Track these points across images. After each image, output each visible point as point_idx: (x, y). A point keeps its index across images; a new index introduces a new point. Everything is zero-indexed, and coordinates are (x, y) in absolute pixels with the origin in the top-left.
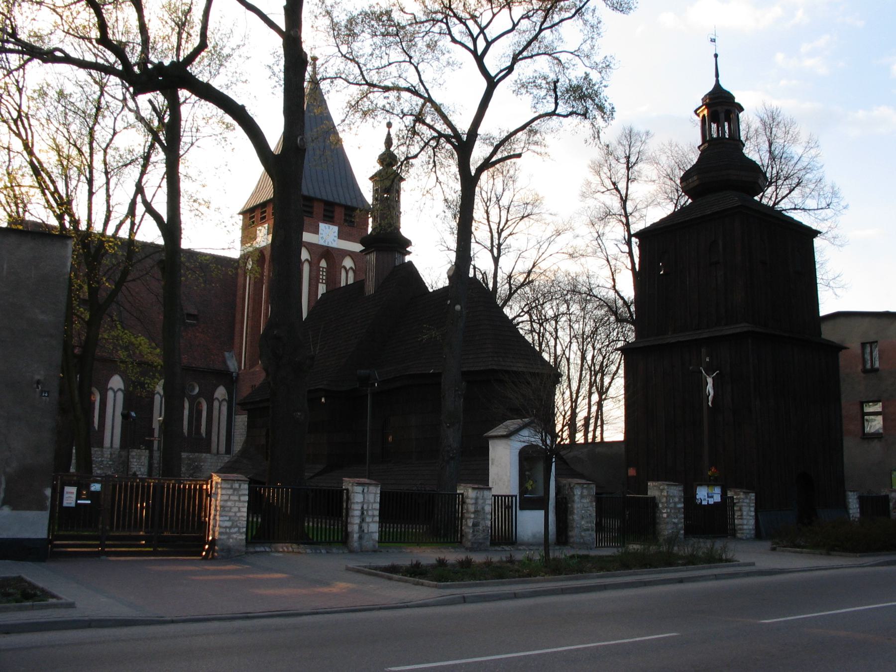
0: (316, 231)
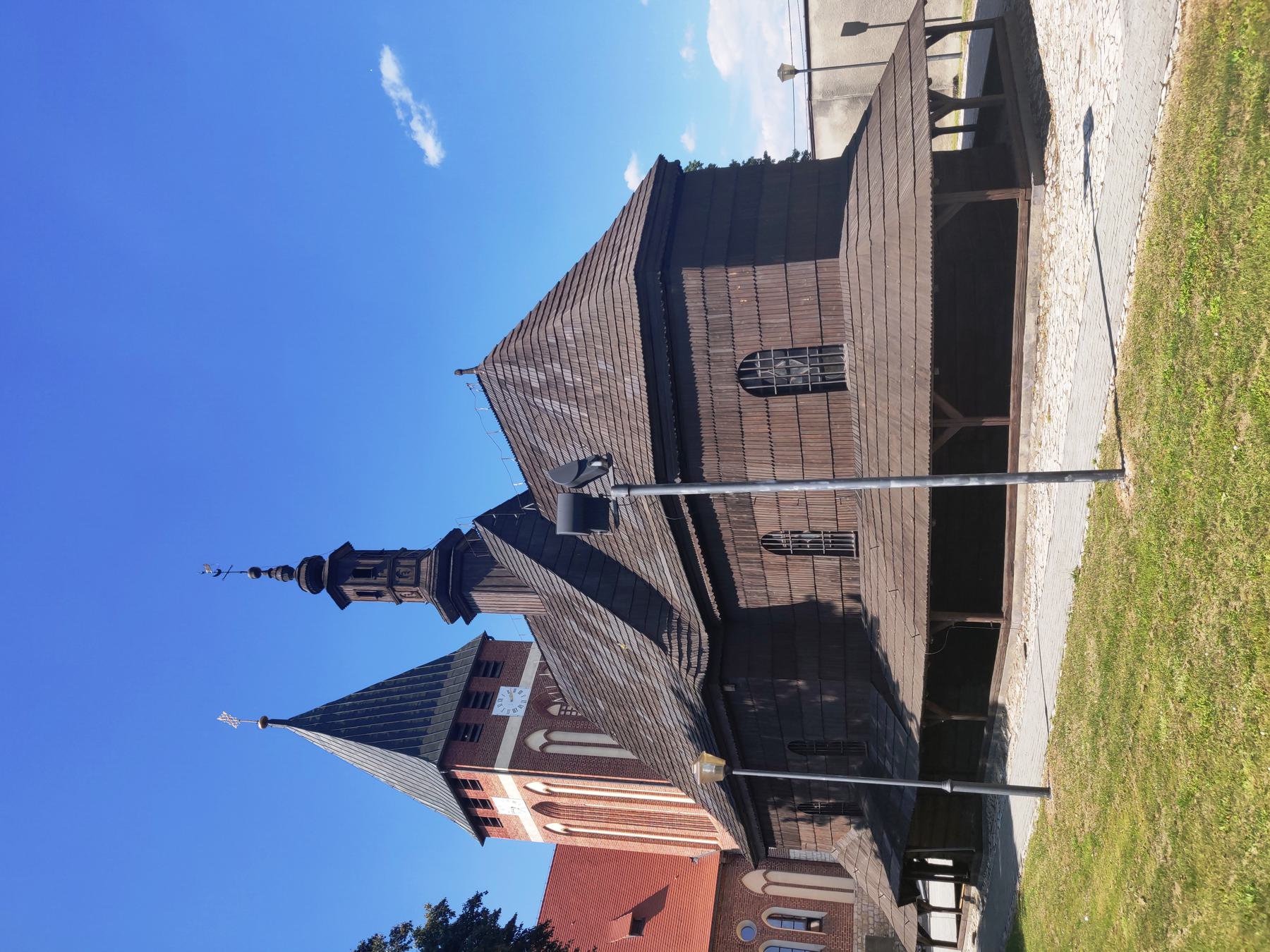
0: (504, 720)
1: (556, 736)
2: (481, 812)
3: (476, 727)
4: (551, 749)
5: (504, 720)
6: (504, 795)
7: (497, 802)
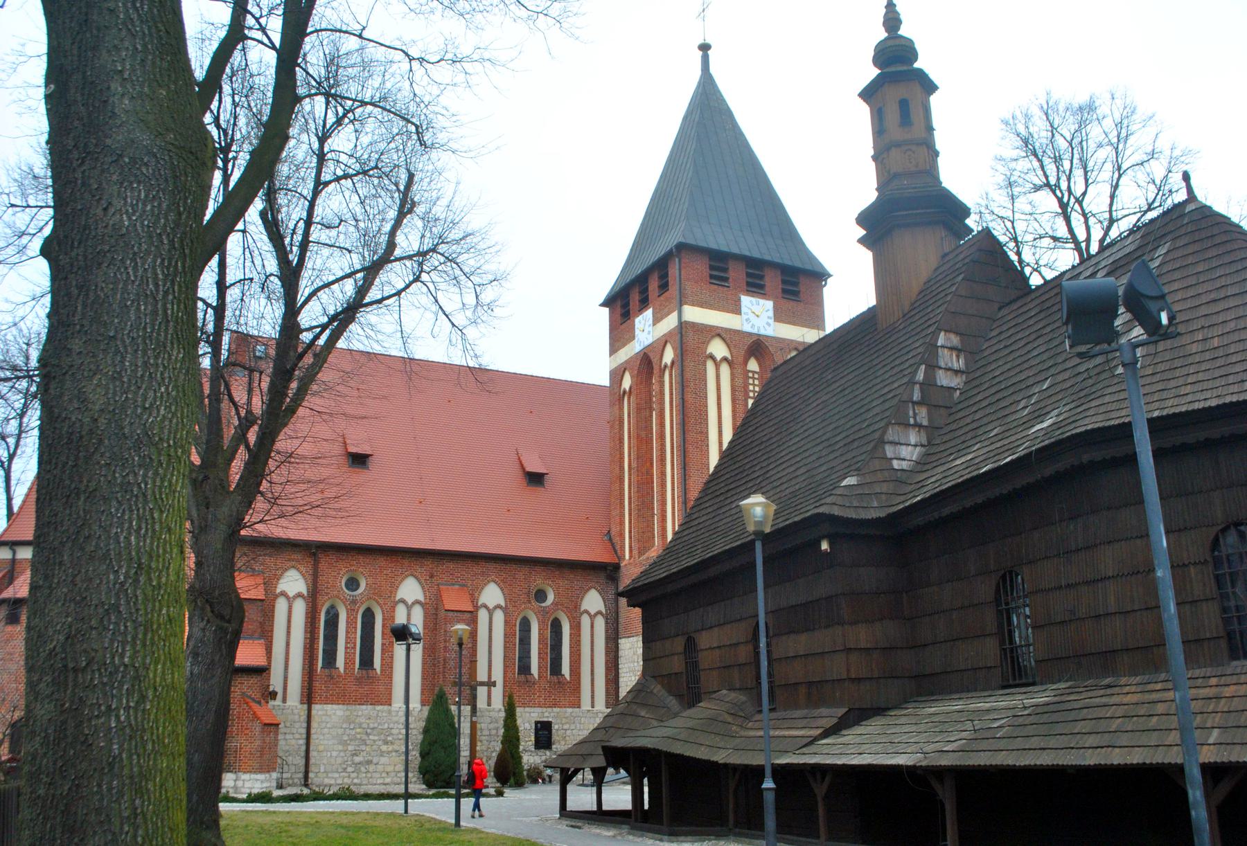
0: (737, 310)
1: (725, 370)
2: (635, 297)
3: (726, 280)
4: (710, 366)
5: (737, 310)
6: (656, 320)
7: (649, 313)
